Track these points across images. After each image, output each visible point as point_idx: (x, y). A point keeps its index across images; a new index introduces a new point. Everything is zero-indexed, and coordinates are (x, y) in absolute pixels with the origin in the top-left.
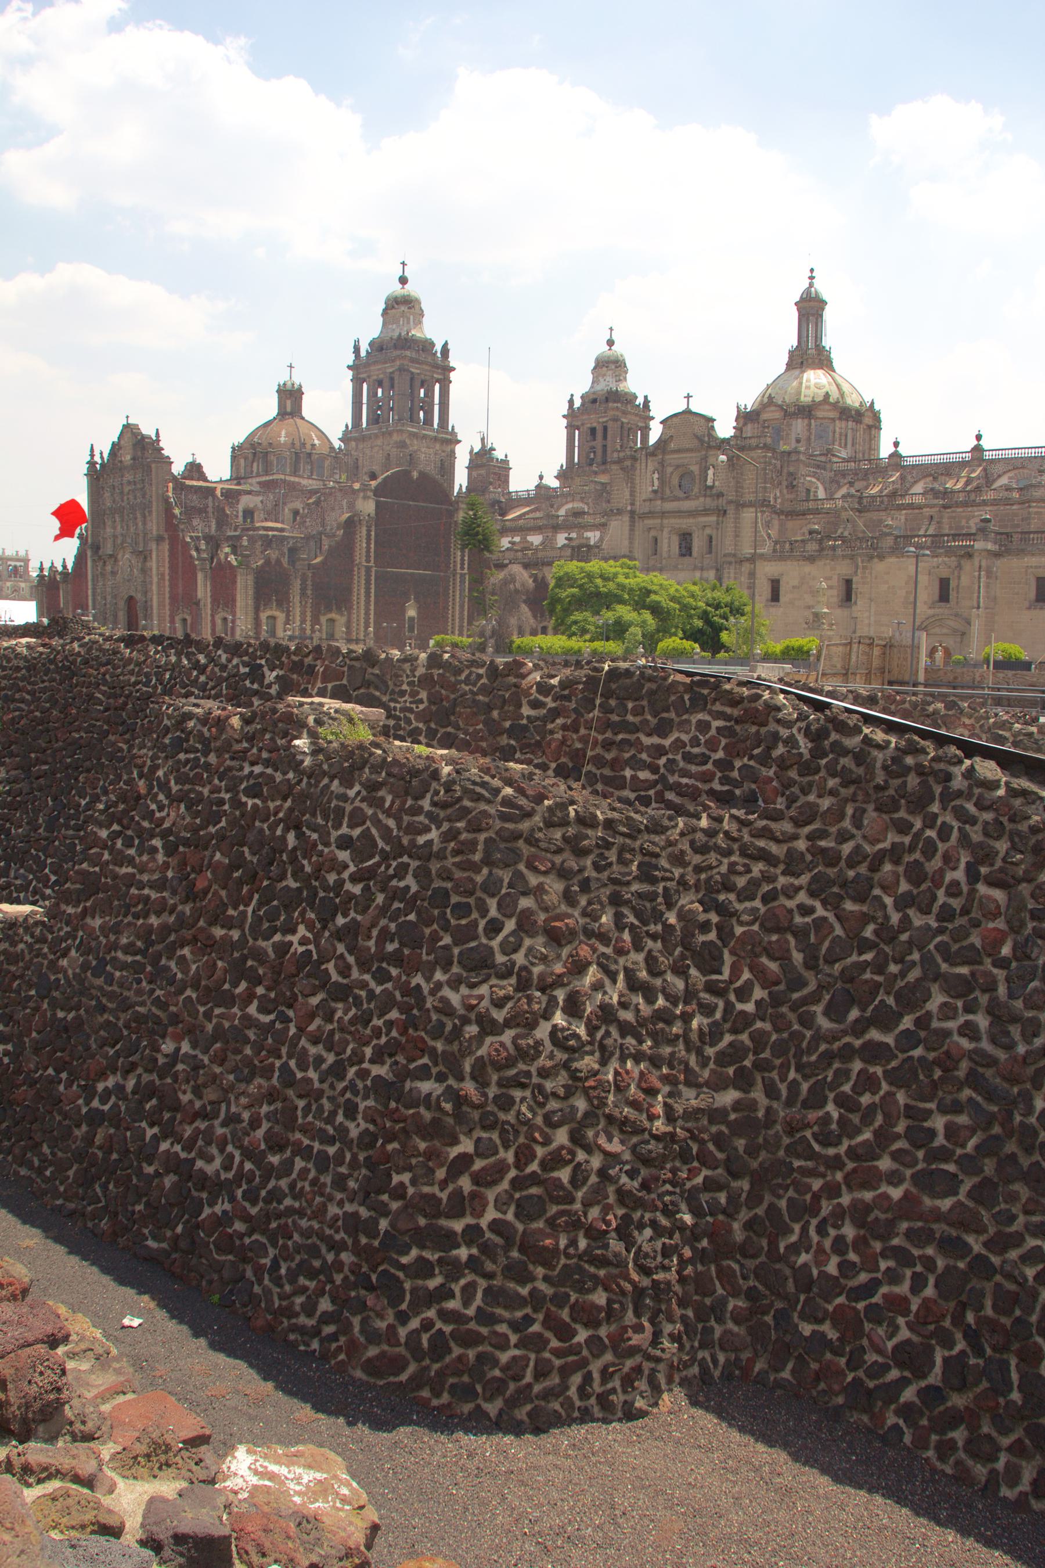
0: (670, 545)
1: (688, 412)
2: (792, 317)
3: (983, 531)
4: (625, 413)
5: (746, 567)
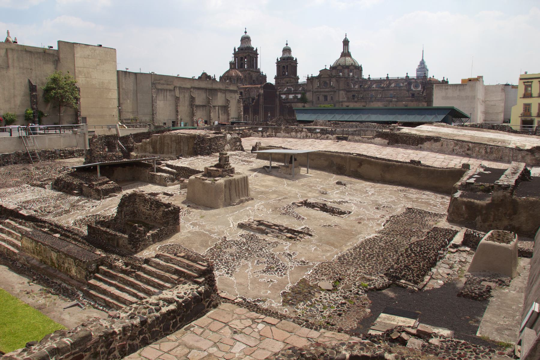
0: (322, 98)
1: (326, 69)
2: (342, 45)
3: (394, 97)
4: (292, 62)
5: (341, 104)
